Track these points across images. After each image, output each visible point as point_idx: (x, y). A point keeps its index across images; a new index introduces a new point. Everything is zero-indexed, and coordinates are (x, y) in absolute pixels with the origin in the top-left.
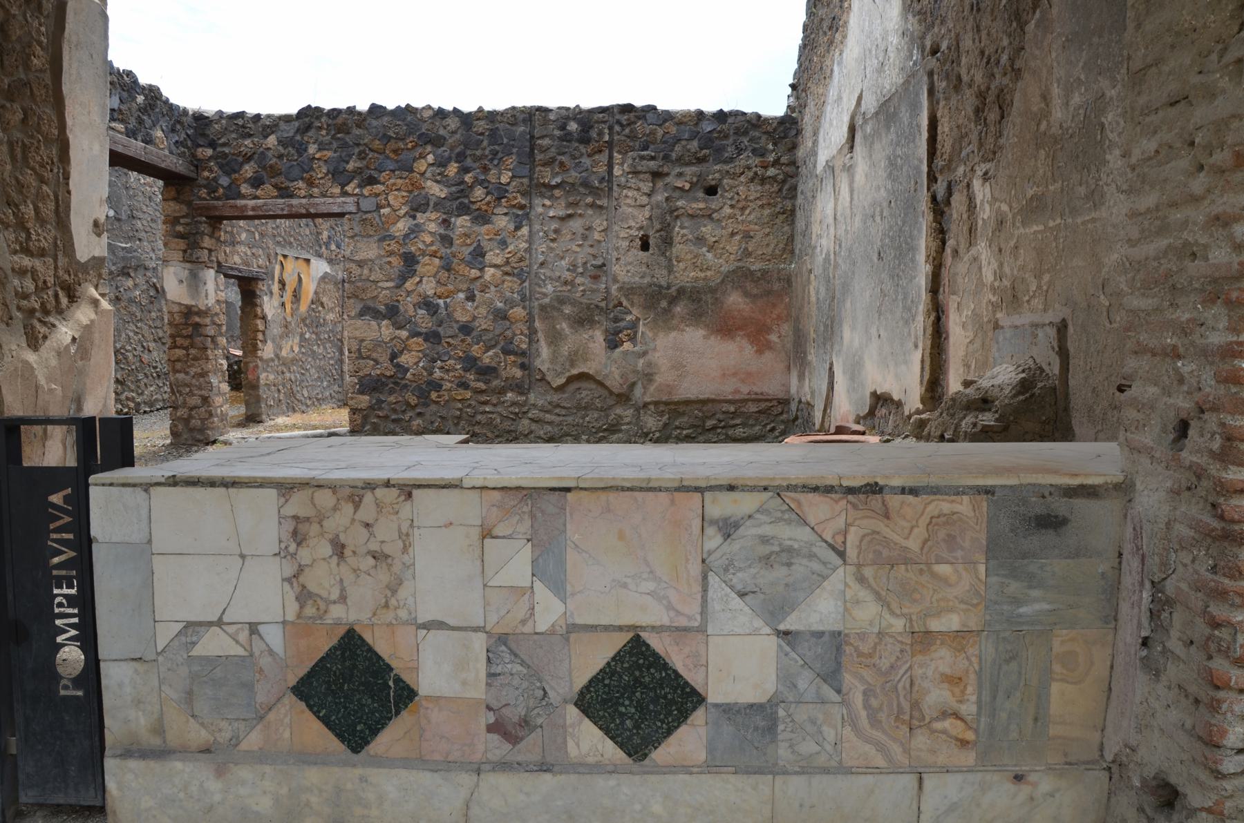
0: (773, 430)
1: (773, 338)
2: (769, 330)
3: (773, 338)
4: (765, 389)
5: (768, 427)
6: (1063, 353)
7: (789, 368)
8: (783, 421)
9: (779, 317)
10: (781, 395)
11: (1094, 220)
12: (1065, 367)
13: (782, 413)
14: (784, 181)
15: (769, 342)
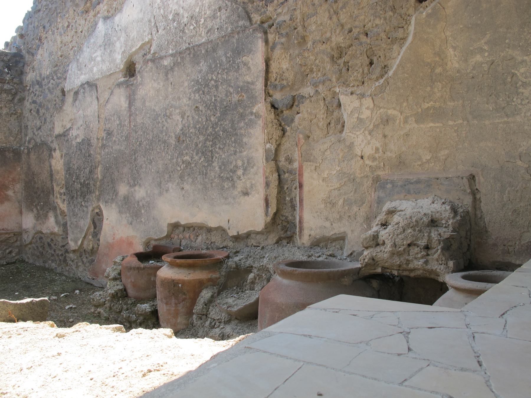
0: (10, 252)
1: (10, 193)
2: (6, 188)
3: (10, 193)
4: (5, 226)
5: (8, 251)
6: (474, 193)
7: (21, 213)
8: (17, 246)
9: (14, 180)
10: (17, 230)
11: (508, 123)
12: (476, 201)
13: (16, 241)
14: (16, 94)
15: (7, 196)
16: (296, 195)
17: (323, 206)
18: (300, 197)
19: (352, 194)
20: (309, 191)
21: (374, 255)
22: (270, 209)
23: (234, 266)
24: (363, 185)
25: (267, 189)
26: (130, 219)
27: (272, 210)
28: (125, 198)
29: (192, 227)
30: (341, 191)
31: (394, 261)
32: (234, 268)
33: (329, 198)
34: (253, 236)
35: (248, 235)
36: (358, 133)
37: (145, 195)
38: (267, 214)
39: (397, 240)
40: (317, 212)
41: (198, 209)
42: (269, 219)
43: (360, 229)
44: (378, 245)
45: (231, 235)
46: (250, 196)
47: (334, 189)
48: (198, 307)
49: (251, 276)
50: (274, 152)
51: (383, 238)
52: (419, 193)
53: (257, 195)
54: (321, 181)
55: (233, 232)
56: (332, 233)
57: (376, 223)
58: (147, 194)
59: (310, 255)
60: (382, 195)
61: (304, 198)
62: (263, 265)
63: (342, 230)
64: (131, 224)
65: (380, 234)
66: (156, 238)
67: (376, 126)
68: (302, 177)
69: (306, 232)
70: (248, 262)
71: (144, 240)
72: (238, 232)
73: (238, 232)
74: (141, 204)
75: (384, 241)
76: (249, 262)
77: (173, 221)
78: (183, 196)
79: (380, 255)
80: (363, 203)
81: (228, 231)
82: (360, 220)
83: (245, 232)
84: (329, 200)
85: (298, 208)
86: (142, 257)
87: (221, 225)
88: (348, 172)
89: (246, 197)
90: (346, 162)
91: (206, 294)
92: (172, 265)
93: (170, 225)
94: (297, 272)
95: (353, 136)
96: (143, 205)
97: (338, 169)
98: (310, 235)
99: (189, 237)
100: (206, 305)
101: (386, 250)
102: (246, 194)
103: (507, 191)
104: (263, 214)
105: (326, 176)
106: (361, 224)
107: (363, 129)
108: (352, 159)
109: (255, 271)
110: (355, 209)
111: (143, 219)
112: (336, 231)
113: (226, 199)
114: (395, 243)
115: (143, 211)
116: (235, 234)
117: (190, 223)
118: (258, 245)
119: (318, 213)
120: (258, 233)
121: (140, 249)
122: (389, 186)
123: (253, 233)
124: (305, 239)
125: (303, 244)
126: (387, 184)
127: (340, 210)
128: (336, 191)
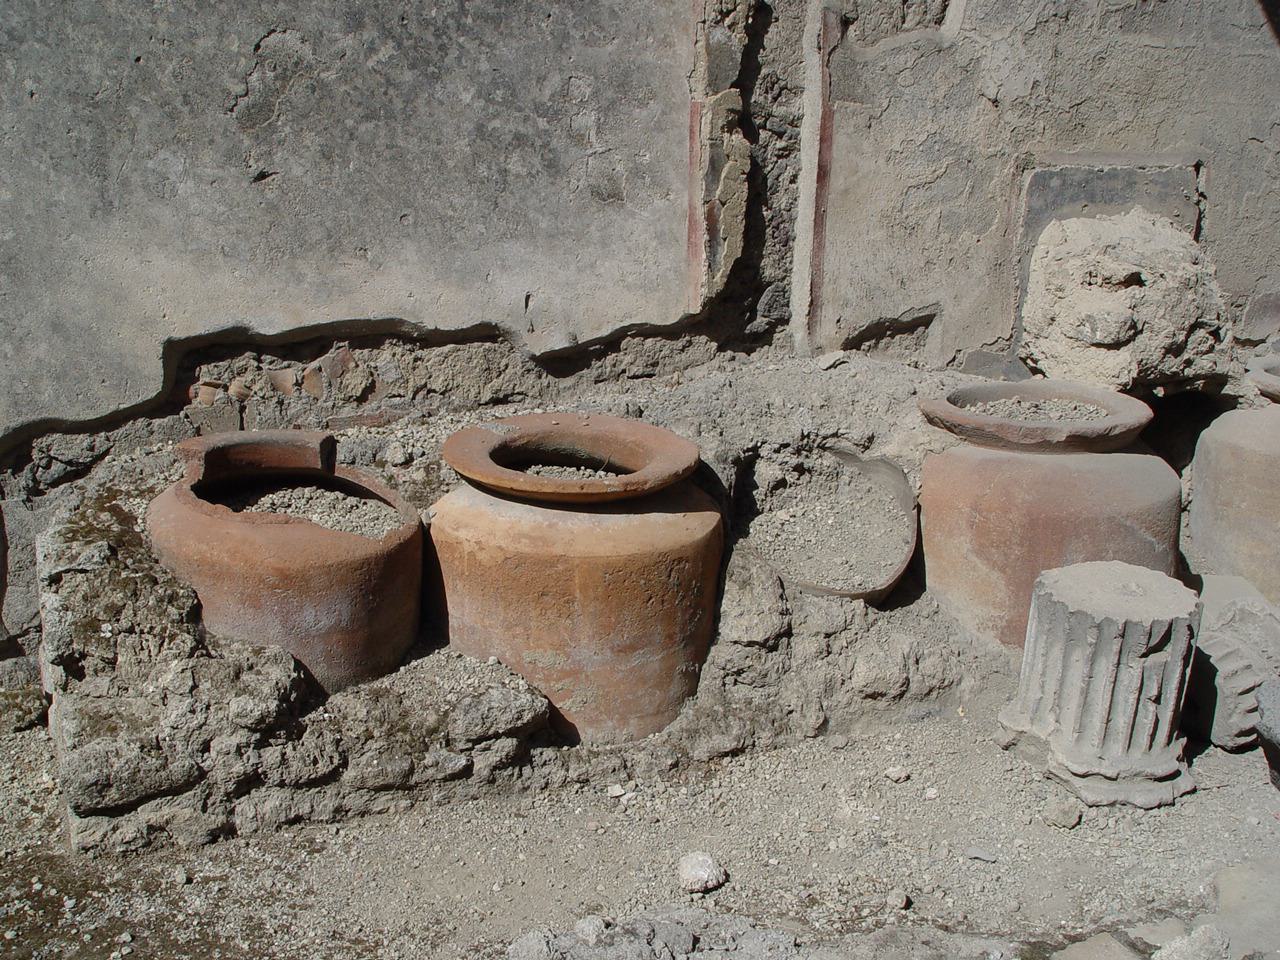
17: (880, 234)
20: (846, 191)
24: (992, 179)
27: (731, 249)
29: (321, 338)
33: (901, 211)
36: (997, 36)
42: (720, 279)
47: (917, 187)
50: (739, 57)
52: (1111, 200)
54: (882, 161)
56: (903, 308)
67: (1041, 23)
68: (830, 147)
88: (957, 141)
90: (953, 111)
94: (1117, 432)
95: (982, 41)
97: (931, 127)
103: (1245, 199)
105: (896, 146)
107: (1010, 28)
108: (969, 105)
110: (966, 236)
122: (1055, 182)
126: (1051, 178)
128: (921, 191)
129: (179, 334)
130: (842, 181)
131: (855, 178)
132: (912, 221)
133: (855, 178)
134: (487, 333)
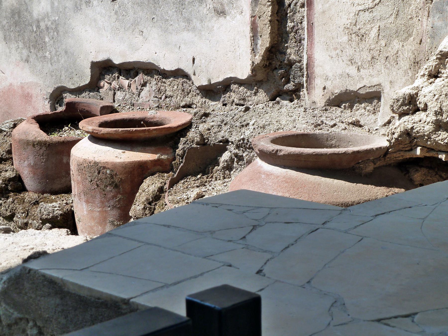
16: (303, 17)
18: (308, 22)
19: (392, 19)
20: (324, 12)
21: (410, 126)
22: (260, 42)
23: (198, 139)
24: (410, 5)
25: (256, 6)
26: (25, 52)
27: (264, 42)
28: (13, 13)
29: (134, 68)
30: (375, 14)
31: (440, 138)
32: (197, 143)
33: (355, 25)
34: (234, 87)
35: (226, 86)
37: (49, 9)
38: (254, 51)
39: (444, 104)
40: (336, 49)
41: (141, 38)
42: (258, 59)
43: (404, 80)
44: (418, 110)
45: (197, 84)
46: (228, 17)
47: (364, 11)
48: (137, 208)
49: (226, 156)
51: (425, 100)
53: (238, 17)
55: (201, 80)
57: (422, 74)
58: (52, 7)
59: (319, 122)
60: (439, 23)
61: (316, 24)
62: (243, 139)
63: (375, 81)
64: (27, 61)
65: (421, 93)
66: (73, 87)
69: (318, 83)
70: (222, 133)
71: (51, 90)
72: (209, 81)
73: (209, 81)
74: (42, 25)
75: (426, 105)
76: (223, 134)
77: (101, 58)
78: (116, 13)
79: (418, 127)
80: (410, 36)
81: (193, 77)
82: (404, 64)
83: (221, 79)
84: (355, 29)
85: (305, 42)
86: (47, 123)
87: (182, 67)
89: (222, 19)
91: (150, 185)
92: (96, 138)
93: (94, 65)
94: (282, 153)
96: (47, 28)
98: (324, 88)
99: (129, 86)
100: (150, 203)
101: (428, 119)
102: (221, 13)
104: (249, 50)
106: (406, 72)
109: (231, 148)
110: (396, 45)
111: (47, 54)
112: (366, 82)
113: (188, 21)
114: (441, 109)
115: (47, 39)
116: (205, 83)
117: (129, 63)
118: (242, 102)
119: (337, 51)
120: (240, 83)
121: (44, 108)
123: (235, 83)
124: (316, 95)
125: (314, 102)
127: (373, 47)
128: (367, 13)
129: (95, 60)
130: (320, 6)
131: (328, 5)
132: (362, 31)
133: (328, 5)
134: (179, 74)
